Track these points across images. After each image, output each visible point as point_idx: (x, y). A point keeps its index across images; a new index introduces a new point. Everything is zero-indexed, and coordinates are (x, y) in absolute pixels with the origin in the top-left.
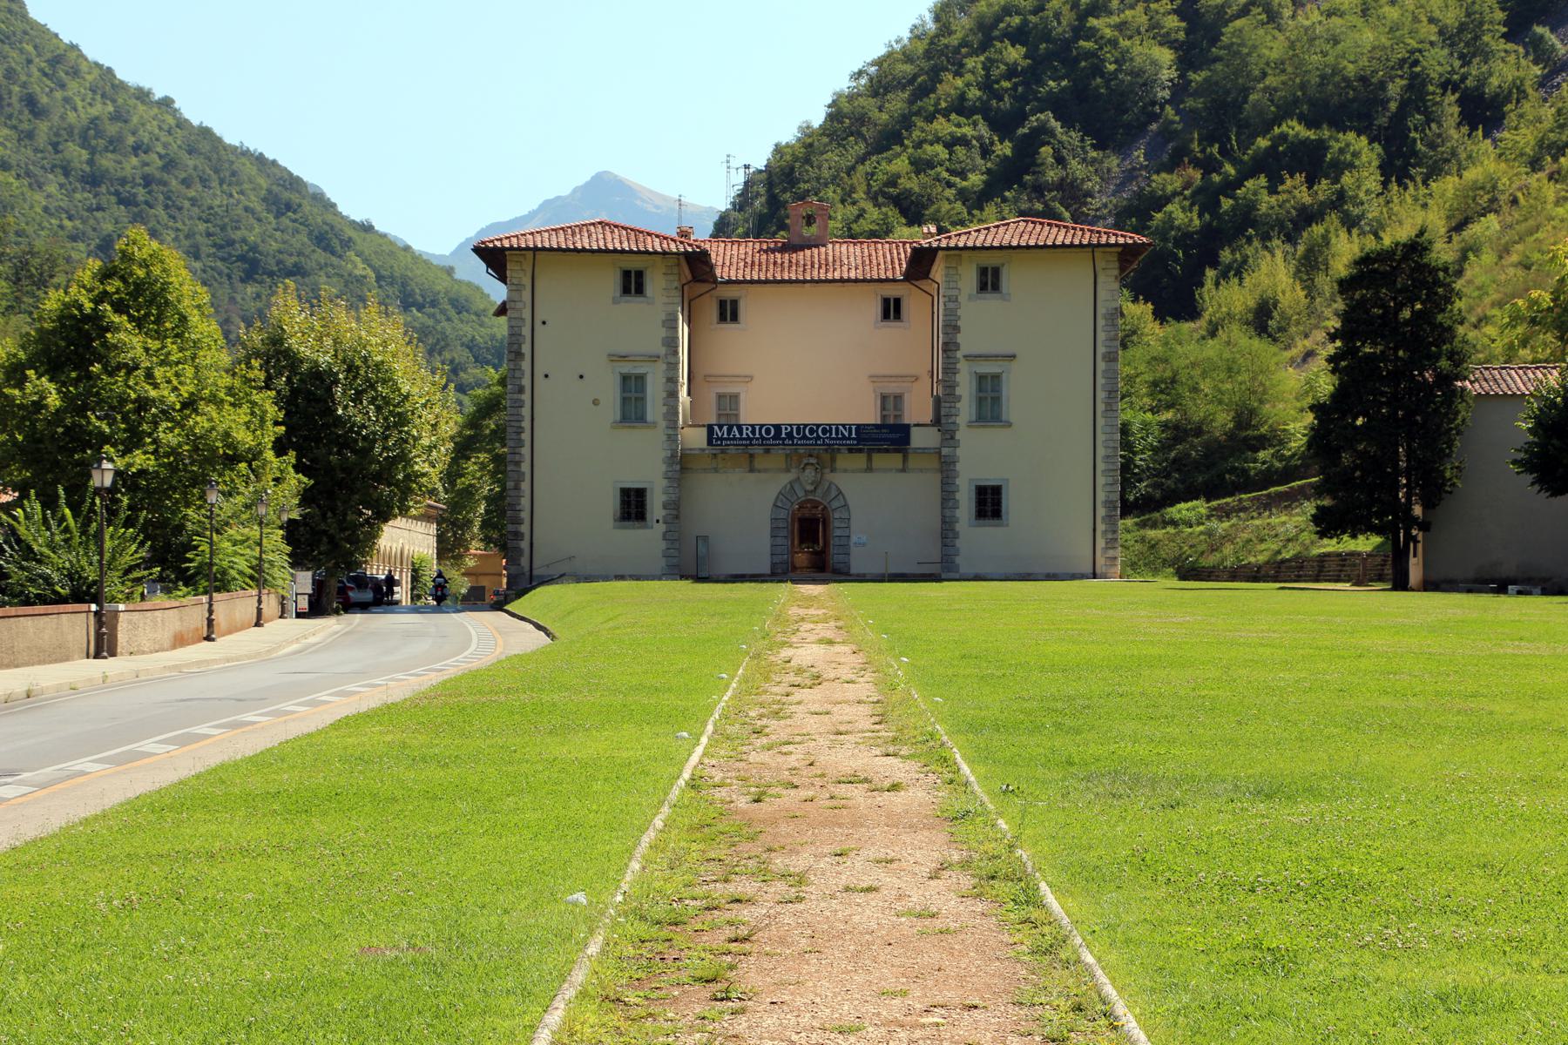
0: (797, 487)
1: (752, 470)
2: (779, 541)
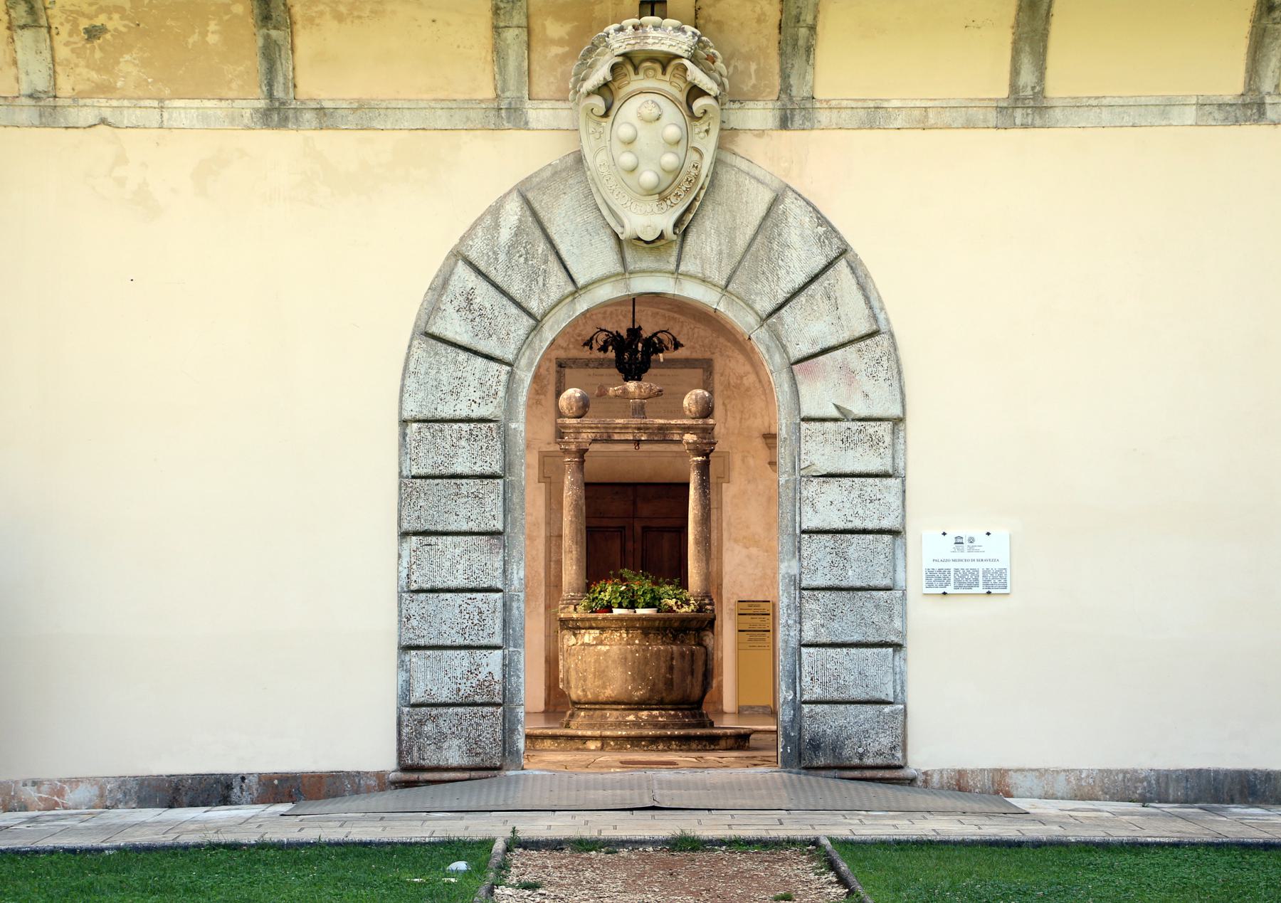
0: (565, 220)
1: (277, 113)
2: (455, 562)
